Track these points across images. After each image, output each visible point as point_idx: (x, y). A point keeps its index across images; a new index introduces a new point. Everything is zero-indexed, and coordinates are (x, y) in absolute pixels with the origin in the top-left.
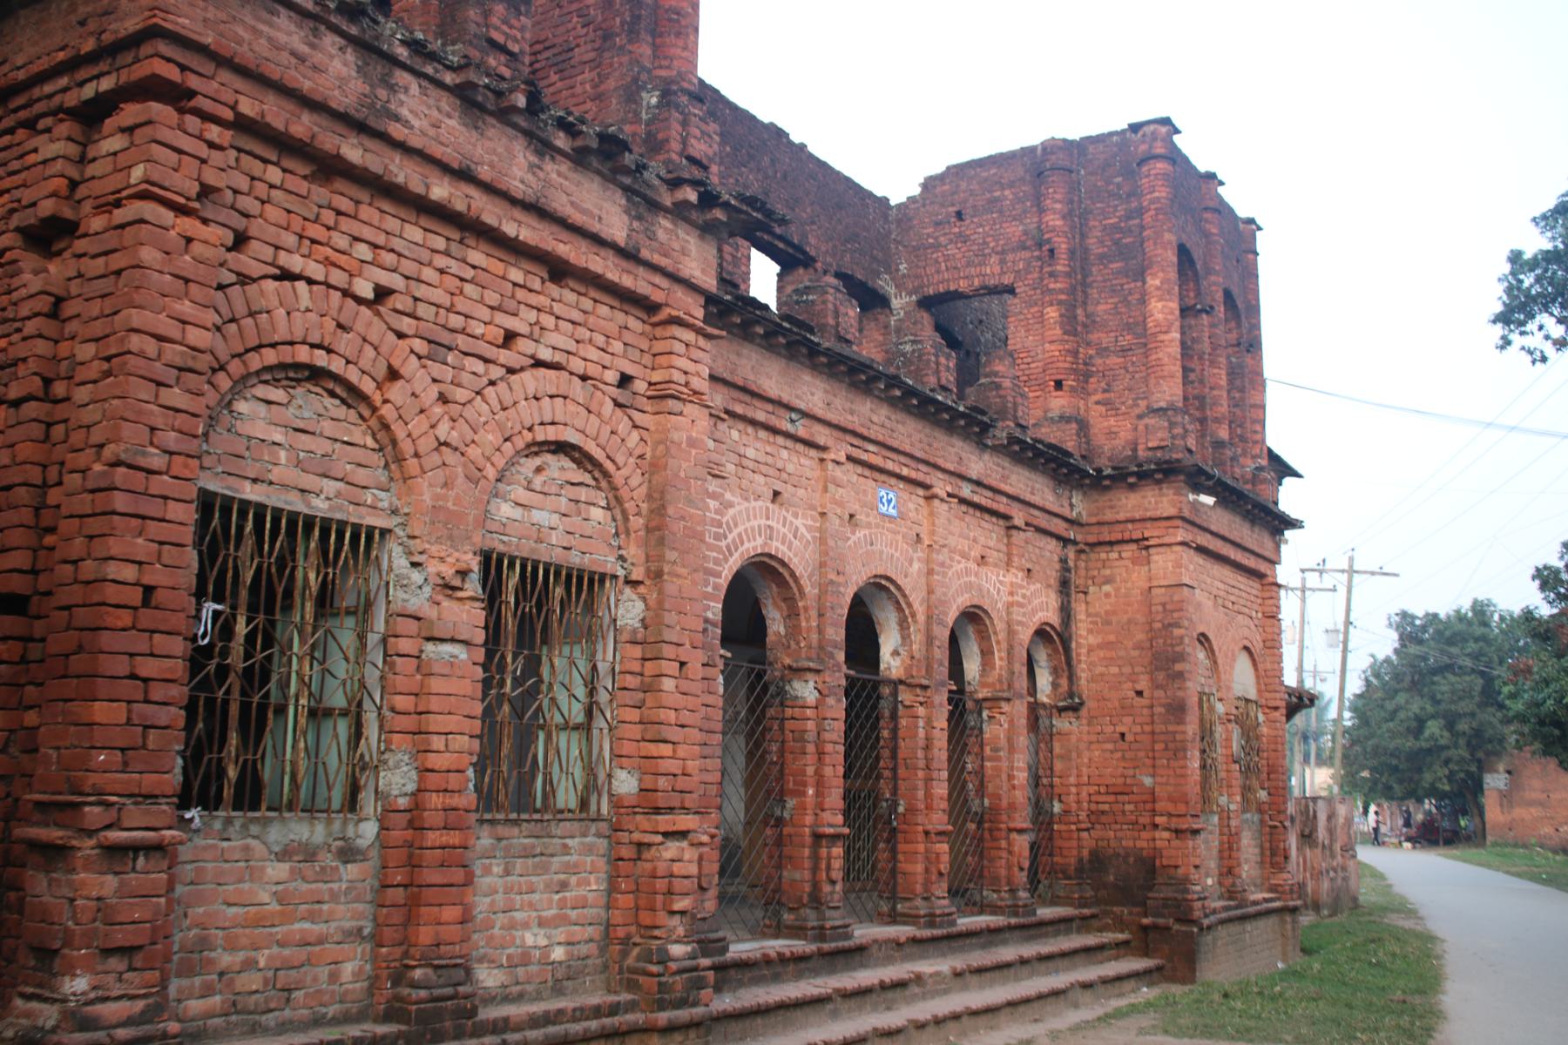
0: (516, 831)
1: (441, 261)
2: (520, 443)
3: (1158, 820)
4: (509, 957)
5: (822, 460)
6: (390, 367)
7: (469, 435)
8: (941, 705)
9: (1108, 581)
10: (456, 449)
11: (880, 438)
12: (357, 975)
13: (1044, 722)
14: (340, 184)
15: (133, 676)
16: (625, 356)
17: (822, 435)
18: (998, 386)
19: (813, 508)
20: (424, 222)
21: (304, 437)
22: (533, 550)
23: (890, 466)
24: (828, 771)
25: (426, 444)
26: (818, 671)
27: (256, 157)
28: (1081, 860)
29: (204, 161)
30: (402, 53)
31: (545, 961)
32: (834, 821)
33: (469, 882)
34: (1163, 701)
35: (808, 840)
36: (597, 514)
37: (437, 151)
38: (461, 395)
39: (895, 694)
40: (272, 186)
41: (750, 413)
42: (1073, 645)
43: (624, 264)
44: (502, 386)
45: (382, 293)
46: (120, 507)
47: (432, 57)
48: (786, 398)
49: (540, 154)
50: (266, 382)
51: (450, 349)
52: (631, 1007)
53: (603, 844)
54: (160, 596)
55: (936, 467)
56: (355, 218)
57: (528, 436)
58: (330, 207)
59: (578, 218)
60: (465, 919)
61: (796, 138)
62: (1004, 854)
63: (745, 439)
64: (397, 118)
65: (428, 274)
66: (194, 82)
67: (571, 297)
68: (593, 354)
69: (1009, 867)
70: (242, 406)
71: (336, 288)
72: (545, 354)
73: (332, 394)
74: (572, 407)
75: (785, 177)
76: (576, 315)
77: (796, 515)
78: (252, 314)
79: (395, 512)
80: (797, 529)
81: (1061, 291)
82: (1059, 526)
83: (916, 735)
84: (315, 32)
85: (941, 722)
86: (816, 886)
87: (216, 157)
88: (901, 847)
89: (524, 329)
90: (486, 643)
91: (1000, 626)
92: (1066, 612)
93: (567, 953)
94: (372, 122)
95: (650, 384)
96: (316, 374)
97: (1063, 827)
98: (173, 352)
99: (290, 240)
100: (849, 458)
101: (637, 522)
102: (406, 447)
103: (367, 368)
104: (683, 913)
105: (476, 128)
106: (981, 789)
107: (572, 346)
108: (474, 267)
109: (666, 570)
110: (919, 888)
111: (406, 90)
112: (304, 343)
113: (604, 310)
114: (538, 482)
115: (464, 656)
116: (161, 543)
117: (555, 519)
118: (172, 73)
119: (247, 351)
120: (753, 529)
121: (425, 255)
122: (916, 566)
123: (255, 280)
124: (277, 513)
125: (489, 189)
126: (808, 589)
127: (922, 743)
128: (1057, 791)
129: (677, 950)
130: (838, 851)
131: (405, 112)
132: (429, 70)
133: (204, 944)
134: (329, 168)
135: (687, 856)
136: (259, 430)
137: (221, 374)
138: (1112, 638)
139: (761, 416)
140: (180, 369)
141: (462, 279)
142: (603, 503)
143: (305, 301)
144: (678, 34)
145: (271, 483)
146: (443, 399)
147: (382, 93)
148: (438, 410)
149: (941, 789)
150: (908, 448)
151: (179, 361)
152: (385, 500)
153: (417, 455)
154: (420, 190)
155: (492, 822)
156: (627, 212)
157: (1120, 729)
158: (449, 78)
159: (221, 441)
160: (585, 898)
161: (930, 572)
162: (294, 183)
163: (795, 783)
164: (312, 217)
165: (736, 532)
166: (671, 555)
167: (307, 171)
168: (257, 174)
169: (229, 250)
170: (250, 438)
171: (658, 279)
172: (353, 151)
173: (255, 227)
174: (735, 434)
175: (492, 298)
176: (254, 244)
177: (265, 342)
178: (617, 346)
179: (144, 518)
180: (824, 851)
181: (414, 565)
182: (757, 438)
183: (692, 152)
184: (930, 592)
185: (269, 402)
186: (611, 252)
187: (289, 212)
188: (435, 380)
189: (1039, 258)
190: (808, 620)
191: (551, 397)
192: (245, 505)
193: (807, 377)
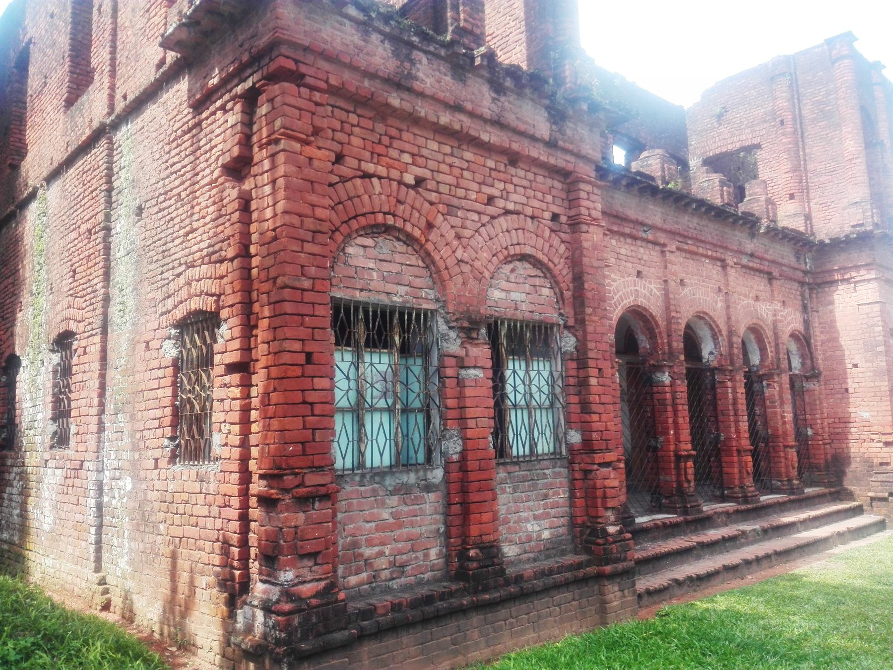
0: (517, 468)
1: (449, 160)
3: (874, 437)
4: (520, 538)
5: (663, 252)
6: (427, 221)
7: (474, 255)
8: (740, 380)
10: (467, 263)
12: (439, 555)
13: (797, 384)
14: (391, 121)
15: (304, 402)
16: (554, 203)
17: (662, 238)
18: (757, 200)
19: (659, 278)
20: (438, 138)
21: (385, 264)
22: (514, 314)
23: (701, 250)
24: (681, 420)
25: (451, 262)
26: (670, 367)
27: (342, 109)
28: (826, 461)
29: (313, 114)
31: (539, 539)
32: (686, 447)
33: (495, 499)
34: (871, 369)
35: (673, 459)
36: (546, 291)
37: (441, 95)
38: (467, 233)
39: (713, 375)
40: (353, 126)
41: (622, 230)
42: (812, 341)
44: (489, 227)
46: (289, 311)
48: (640, 218)
50: (361, 236)
51: (459, 208)
52: (589, 563)
53: (564, 471)
54: (315, 357)
55: (726, 248)
56: (400, 139)
57: (506, 253)
58: (386, 135)
59: (522, 127)
60: (495, 518)
62: (783, 460)
64: (416, 78)
65: (443, 167)
66: (303, 69)
67: (521, 173)
68: (536, 204)
69: (787, 467)
71: (394, 180)
72: (511, 206)
73: (399, 239)
74: (527, 235)
76: (525, 183)
77: (650, 283)
78: (350, 199)
79: (437, 300)
80: (652, 290)
81: (790, 143)
82: (800, 275)
83: (727, 398)
85: (741, 390)
86: (680, 484)
87: (320, 110)
88: (724, 459)
89: (497, 193)
90: (493, 366)
91: (770, 333)
92: (807, 323)
93: (551, 534)
94: (403, 82)
95: (569, 217)
96: (387, 229)
97: (814, 443)
98: (309, 223)
99: (367, 155)
100: (678, 249)
101: (568, 294)
102: (441, 265)
103: (416, 223)
104: (613, 508)
105: (461, 80)
106: (766, 424)
107: (524, 200)
108: (468, 161)
109: (587, 318)
110: (737, 482)
111: (420, 62)
112: (380, 212)
113: (540, 179)
114: (512, 277)
115: (481, 375)
116: (313, 328)
118: (291, 65)
119: (350, 219)
121: (440, 157)
123: (350, 179)
124: (376, 305)
125: (472, 115)
126: (660, 323)
127: (731, 401)
128: (808, 422)
130: (690, 464)
133: (355, 545)
134: (384, 112)
135: (612, 476)
136: (360, 262)
137: (337, 233)
139: (627, 230)
140: (314, 232)
141: (462, 169)
142: (549, 285)
143: (378, 189)
145: (370, 290)
146: (458, 237)
147: (407, 65)
149: (744, 426)
150: (711, 240)
151: (312, 227)
152: (432, 294)
153: (447, 268)
154: (435, 120)
155: (502, 464)
156: (548, 120)
159: (341, 270)
160: (557, 502)
161: (728, 307)
162: (365, 123)
163: (662, 428)
164: (377, 141)
166: (589, 311)
167: (371, 114)
168: (344, 119)
169: (333, 164)
170: (356, 267)
171: (568, 158)
172: (395, 101)
174: (614, 242)
176: (348, 159)
177: (359, 213)
178: (549, 198)
179: (302, 315)
181: (451, 328)
182: (625, 243)
184: (729, 318)
185: (365, 247)
187: (364, 139)
188: (452, 227)
189: (774, 126)
190: (662, 338)
191: (516, 230)
192: (357, 305)
193: (652, 207)
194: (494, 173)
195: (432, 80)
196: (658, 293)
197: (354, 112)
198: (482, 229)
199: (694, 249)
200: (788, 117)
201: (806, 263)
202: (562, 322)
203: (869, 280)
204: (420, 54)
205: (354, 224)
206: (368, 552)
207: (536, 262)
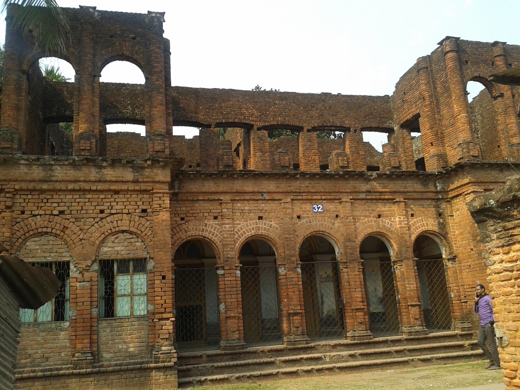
0: (114, 321)
2: (106, 234)
8: (354, 267)
9: (458, 210)
11: (307, 190)
14: (47, 193)
17: (277, 196)
19: (279, 217)
30: (53, 162)
37: (67, 179)
41: (242, 198)
42: (449, 235)
43: (136, 184)
45: (62, 212)
47: (60, 161)
48: (256, 190)
49: (99, 169)
61: (334, 92)
63: (243, 205)
64: (54, 176)
66: (4, 187)
68: (130, 207)
70: (28, 244)
72: (113, 211)
75: (330, 107)
76: (124, 200)
79: (71, 256)
81: (428, 111)
82: (431, 195)
84: (30, 167)
89: (106, 208)
96: (46, 233)
99: (35, 208)
111: (57, 169)
117: (123, 248)
120: (250, 229)
122: (337, 225)
129: (164, 348)
131: (56, 174)
132: (61, 163)
134: (42, 191)
138: (462, 231)
142: (141, 241)
144: (154, 121)
147: (49, 172)
148: (80, 232)
152: (68, 254)
154: (66, 188)
157: (469, 264)
158: (67, 163)
165: (242, 231)
171: (148, 184)
172: (45, 186)
173: (25, 209)
175: (94, 204)
180: (291, 318)
181: (75, 267)
183: (155, 150)
186: (130, 183)
193: (266, 182)
194: (104, 200)
195: (62, 174)
196: (277, 226)
197: (31, 194)
198: (96, 225)
199: (309, 197)
200: (426, 94)
201: (436, 187)
202: (148, 256)
203: (469, 194)
204: (57, 166)
205: (27, 235)
206: (30, 352)
207: (131, 233)
